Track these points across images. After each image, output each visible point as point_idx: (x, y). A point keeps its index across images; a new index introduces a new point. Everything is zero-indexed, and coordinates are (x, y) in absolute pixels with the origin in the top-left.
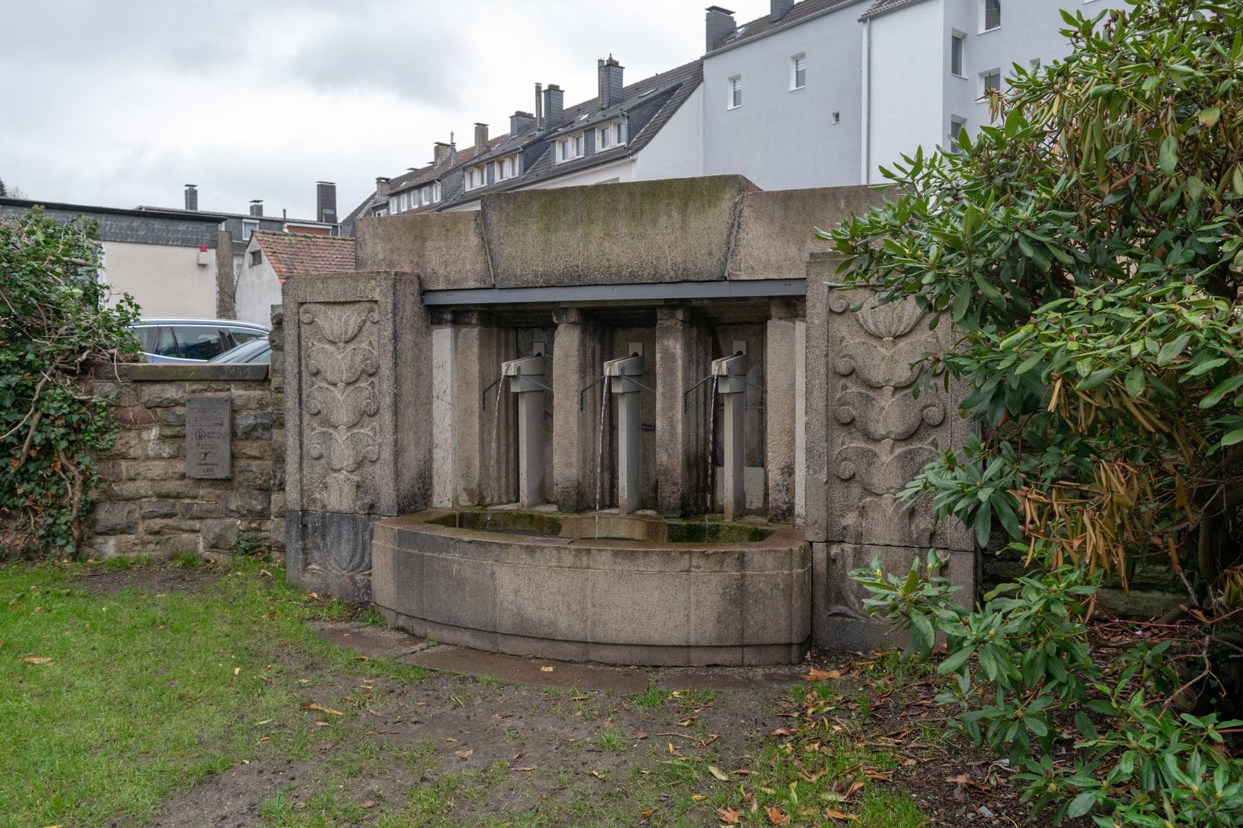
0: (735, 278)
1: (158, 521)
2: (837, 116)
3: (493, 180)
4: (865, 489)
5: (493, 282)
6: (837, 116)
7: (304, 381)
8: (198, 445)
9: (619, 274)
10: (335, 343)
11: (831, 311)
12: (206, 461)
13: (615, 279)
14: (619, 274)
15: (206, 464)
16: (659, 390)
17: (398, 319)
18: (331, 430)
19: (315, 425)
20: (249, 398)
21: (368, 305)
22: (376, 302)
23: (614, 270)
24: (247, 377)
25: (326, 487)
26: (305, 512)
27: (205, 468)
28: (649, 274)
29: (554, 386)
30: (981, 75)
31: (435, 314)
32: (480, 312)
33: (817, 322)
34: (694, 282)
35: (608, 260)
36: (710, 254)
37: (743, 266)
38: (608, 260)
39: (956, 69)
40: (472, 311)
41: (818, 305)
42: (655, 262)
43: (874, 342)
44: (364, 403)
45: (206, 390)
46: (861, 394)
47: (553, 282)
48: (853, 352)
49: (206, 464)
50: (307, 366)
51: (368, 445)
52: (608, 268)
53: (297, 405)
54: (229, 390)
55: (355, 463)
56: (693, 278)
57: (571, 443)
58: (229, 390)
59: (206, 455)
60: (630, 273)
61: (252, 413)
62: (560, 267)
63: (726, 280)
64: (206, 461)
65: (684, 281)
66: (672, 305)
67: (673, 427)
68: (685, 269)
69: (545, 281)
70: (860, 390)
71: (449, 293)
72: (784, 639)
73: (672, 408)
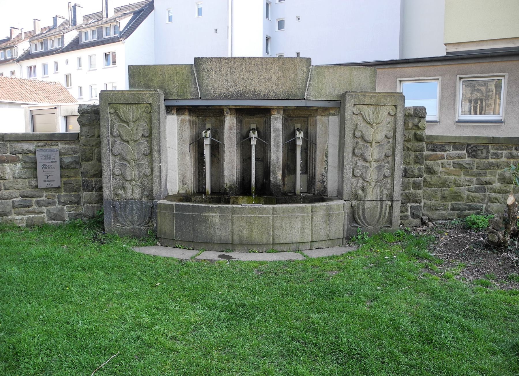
0: (308, 99)
1: (22, 209)
2: (216, 30)
3: (47, 48)
4: (364, 180)
5: (200, 96)
6: (216, 30)
7: (110, 140)
8: (44, 172)
9: (259, 95)
10: (128, 122)
11: (354, 114)
12: (48, 179)
13: (258, 97)
14: (259, 95)
15: (48, 181)
16: (272, 143)
17: (160, 111)
18: (125, 163)
19: (117, 161)
20: (68, 149)
21: (145, 105)
22: (150, 103)
23: (257, 93)
24: (68, 139)
25: (123, 187)
26: (113, 201)
27: (48, 183)
28: (273, 95)
29: (225, 142)
30: (277, 19)
31: (169, 109)
32: (188, 109)
33: (349, 118)
34: (292, 100)
35: (254, 89)
36: (299, 89)
37: (312, 94)
38: (254, 89)
39: (267, 16)
40: (185, 109)
41: (349, 111)
42: (275, 91)
43: (369, 126)
44: (143, 149)
45: (45, 145)
46: (364, 145)
47: (229, 97)
48: (362, 129)
49: (48, 181)
50: (112, 134)
51: (146, 169)
52: (254, 92)
53: (108, 151)
54: (57, 145)
55: (139, 177)
56: (291, 98)
57: (233, 166)
58: (57, 145)
59: (48, 176)
60: (264, 95)
61: (69, 156)
62: (232, 90)
63: (304, 99)
64: (48, 179)
65: (287, 99)
66: (278, 108)
67: (278, 159)
68: (288, 94)
69: (225, 97)
70: (363, 143)
71: (177, 100)
72: (342, 236)
73: (277, 151)
